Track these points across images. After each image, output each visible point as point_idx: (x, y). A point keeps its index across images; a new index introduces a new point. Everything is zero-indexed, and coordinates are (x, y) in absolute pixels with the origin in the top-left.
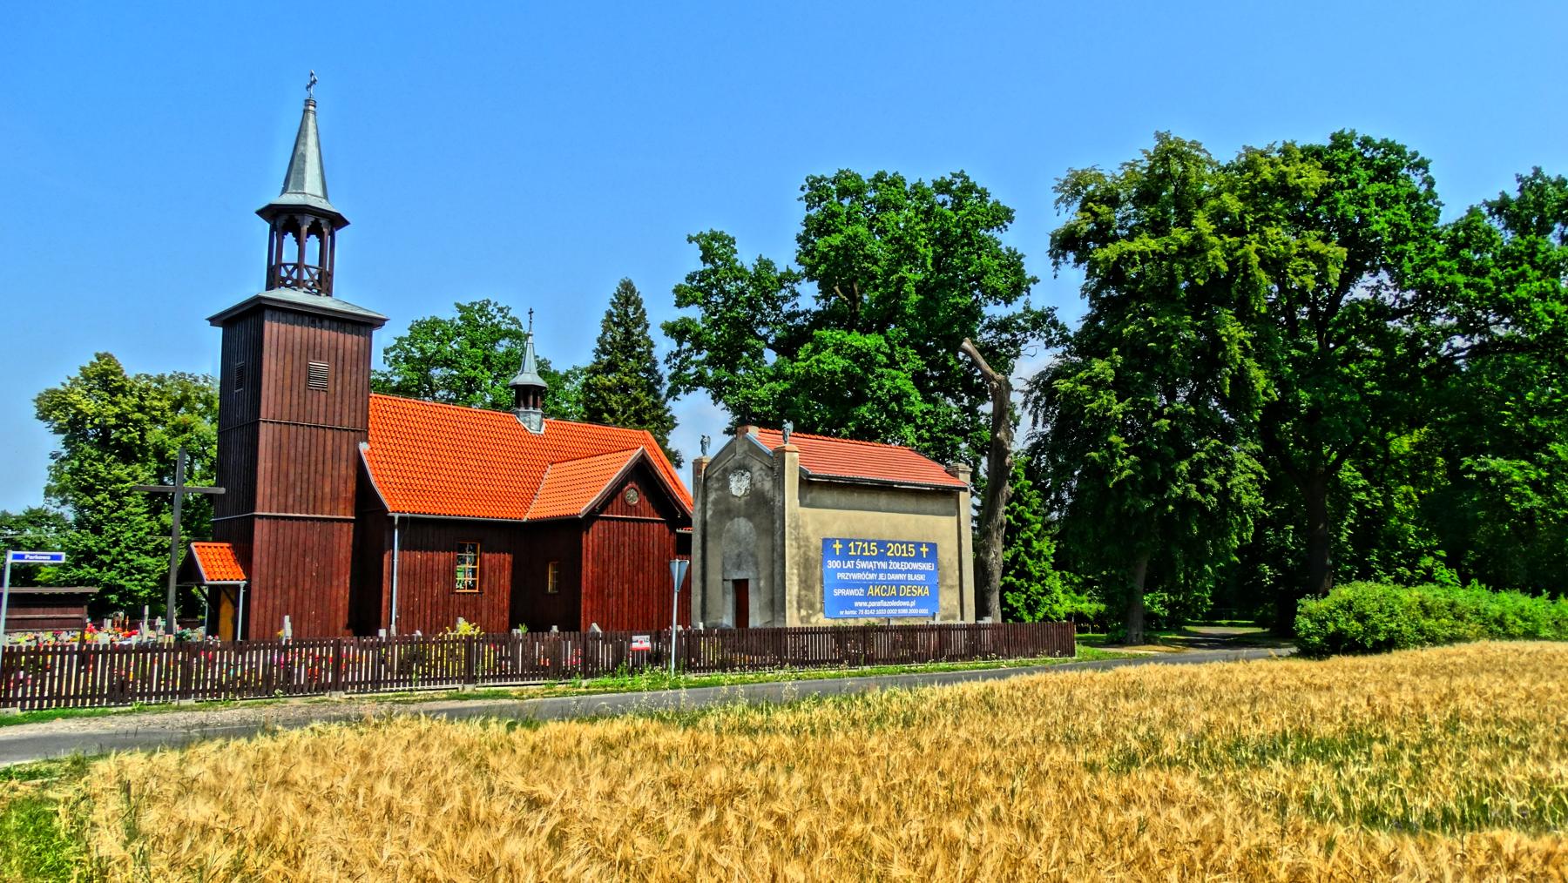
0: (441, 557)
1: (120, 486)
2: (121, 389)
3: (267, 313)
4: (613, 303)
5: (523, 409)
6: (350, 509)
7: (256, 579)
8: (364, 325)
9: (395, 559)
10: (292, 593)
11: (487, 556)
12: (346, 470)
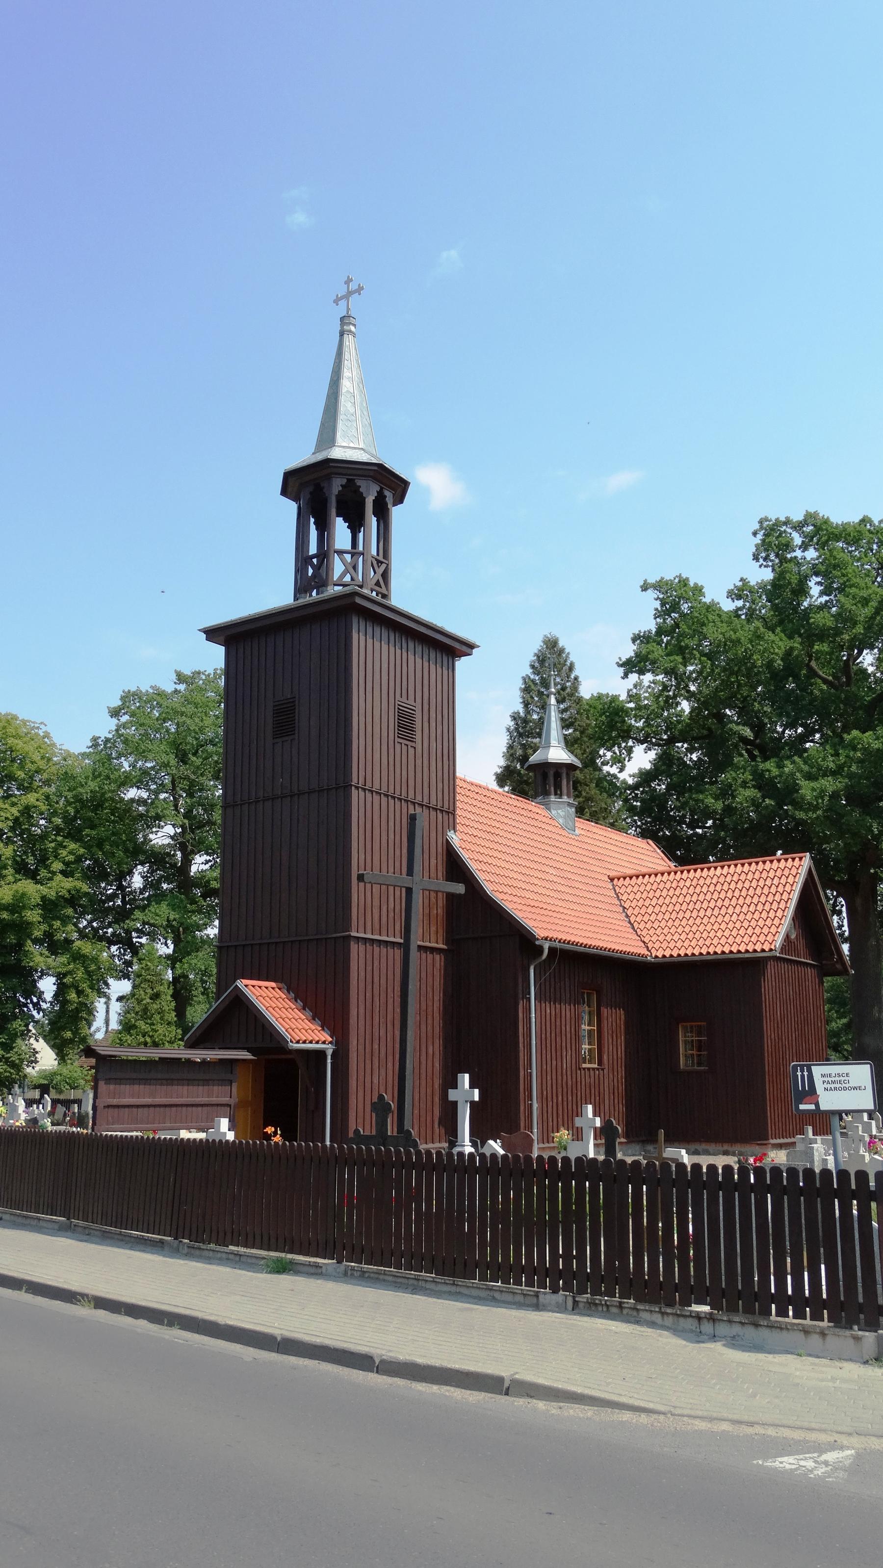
0: (567, 1010)
4: (533, 667)
5: (553, 798)
9: (534, 1013)
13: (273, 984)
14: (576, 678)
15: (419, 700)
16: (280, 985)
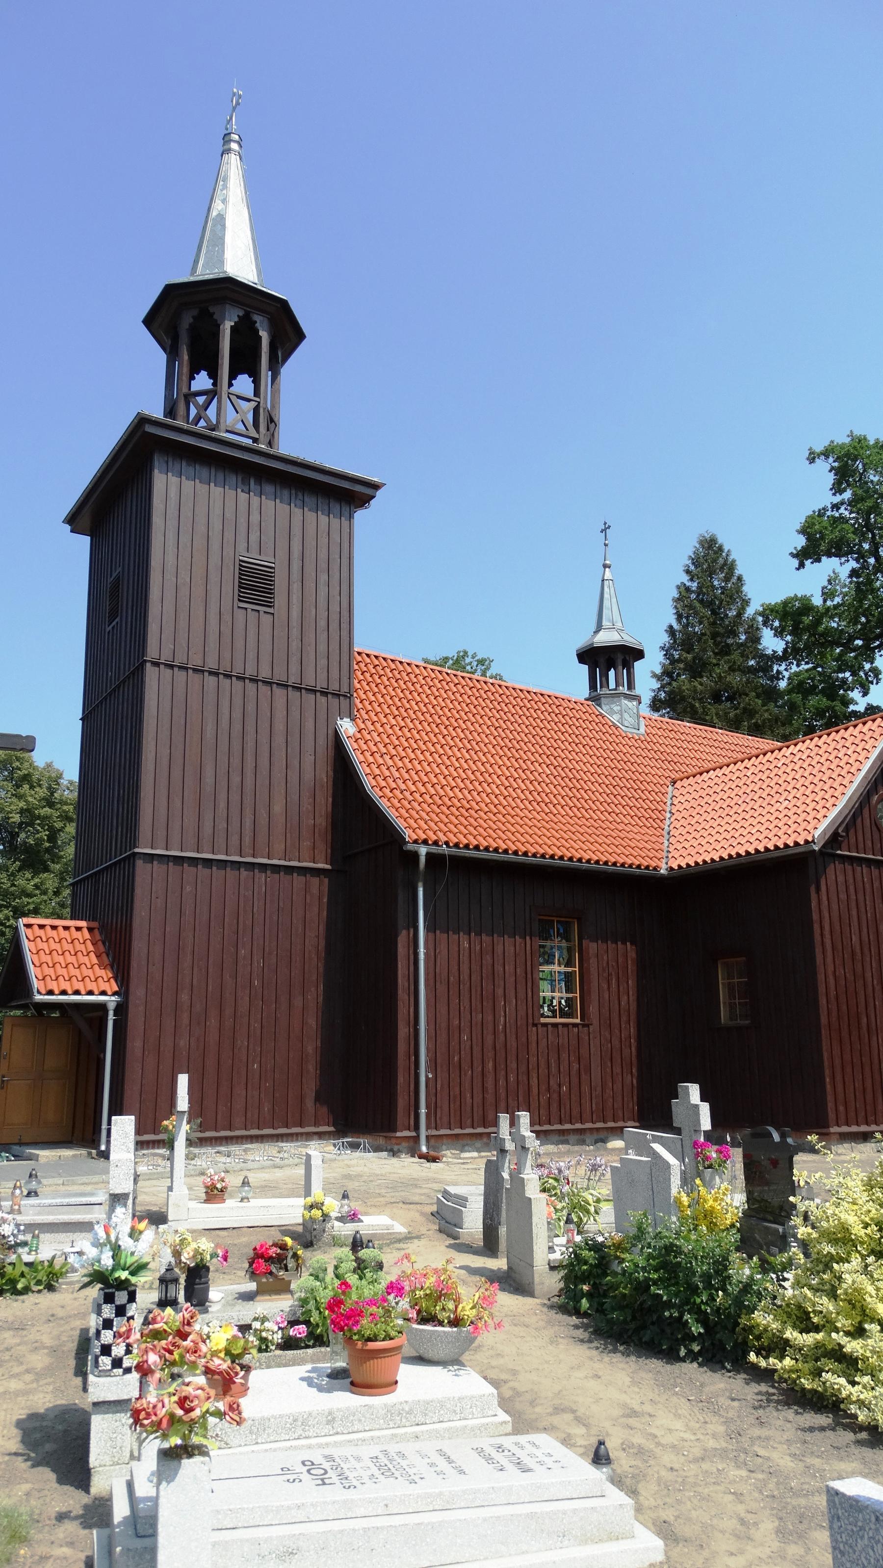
0: (508, 946)
1: (26, 900)
2: (26, 778)
3: (158, 462)
4: (688, 572)
6: (323, 849)
7: (138, 992)
8: (346, 494)
10: (213, 1022)
11: (592, 947)
12: (316, 769)
13: (83, 924)
14: (740, 579)
15: (282, 554)
16: (95, 924)
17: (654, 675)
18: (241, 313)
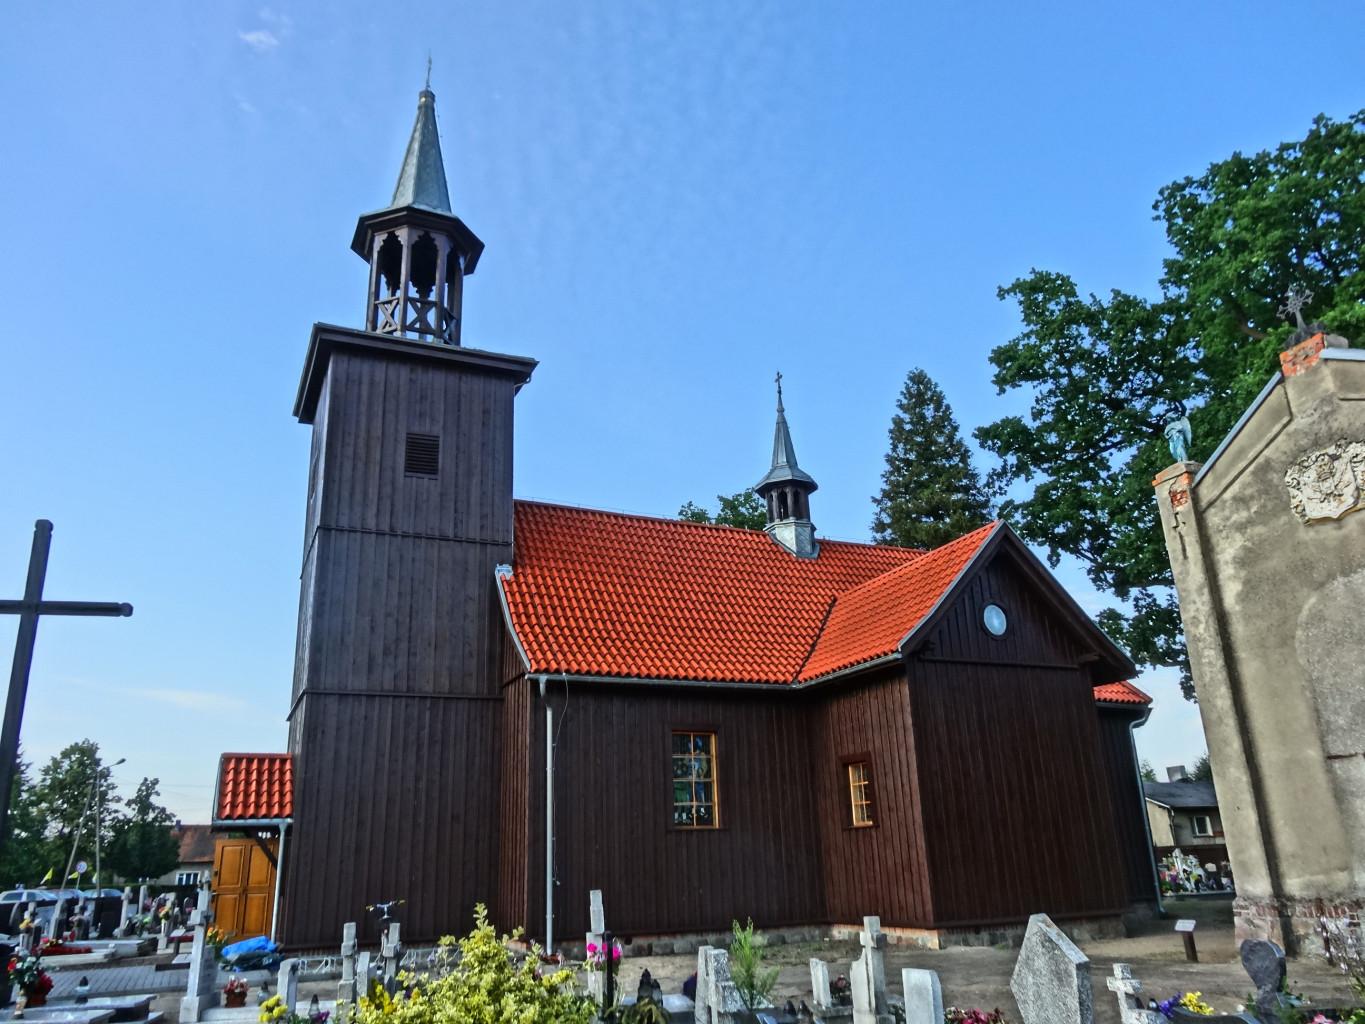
14: (948, 407)
17: (875, 500)
18: (421, 233)
